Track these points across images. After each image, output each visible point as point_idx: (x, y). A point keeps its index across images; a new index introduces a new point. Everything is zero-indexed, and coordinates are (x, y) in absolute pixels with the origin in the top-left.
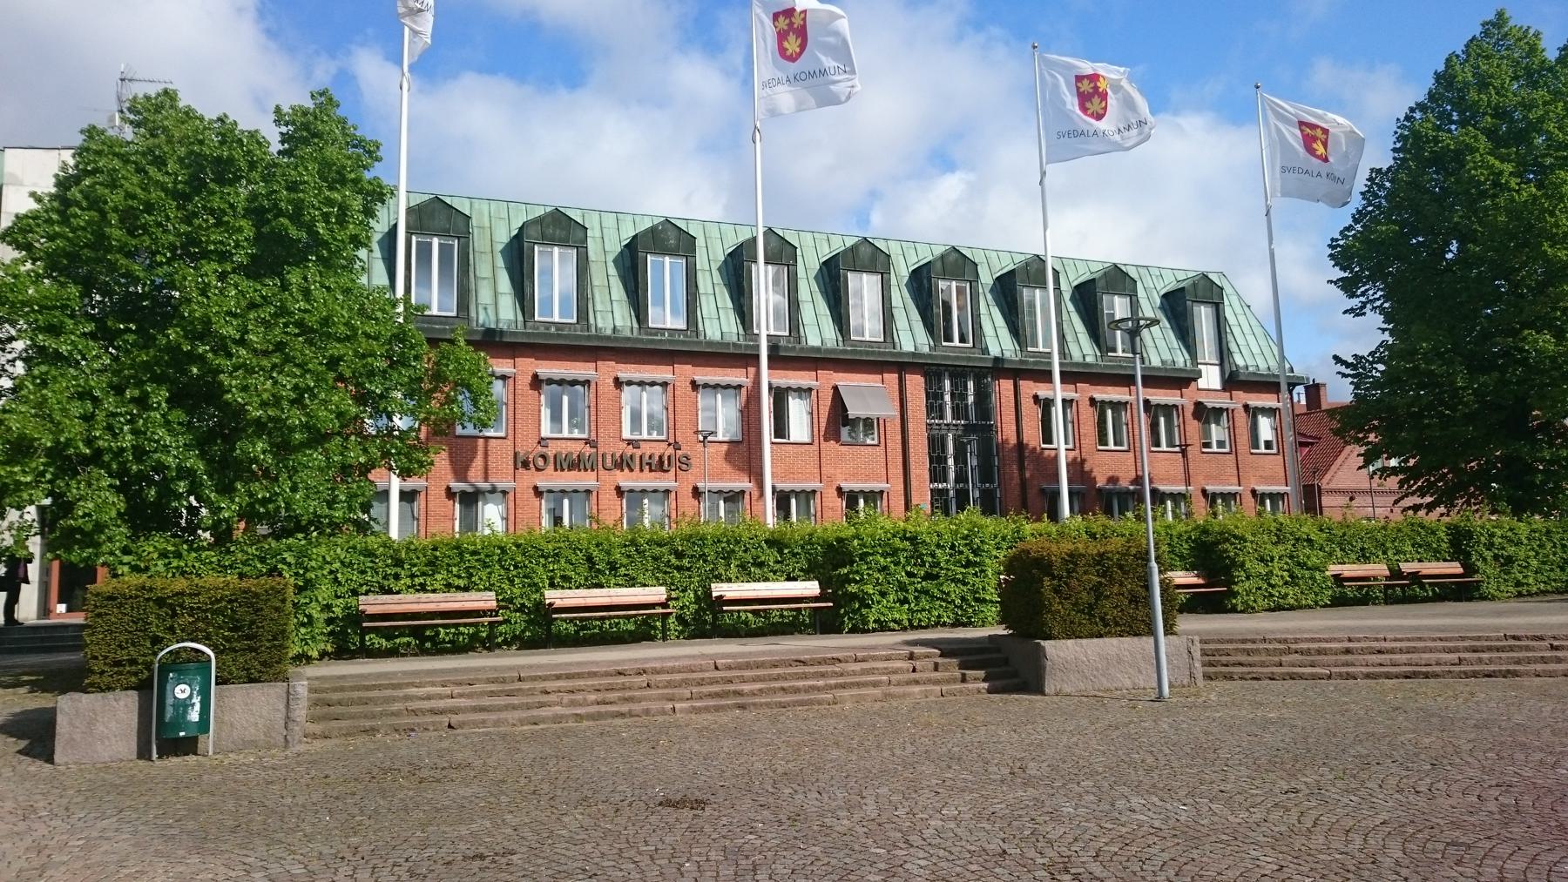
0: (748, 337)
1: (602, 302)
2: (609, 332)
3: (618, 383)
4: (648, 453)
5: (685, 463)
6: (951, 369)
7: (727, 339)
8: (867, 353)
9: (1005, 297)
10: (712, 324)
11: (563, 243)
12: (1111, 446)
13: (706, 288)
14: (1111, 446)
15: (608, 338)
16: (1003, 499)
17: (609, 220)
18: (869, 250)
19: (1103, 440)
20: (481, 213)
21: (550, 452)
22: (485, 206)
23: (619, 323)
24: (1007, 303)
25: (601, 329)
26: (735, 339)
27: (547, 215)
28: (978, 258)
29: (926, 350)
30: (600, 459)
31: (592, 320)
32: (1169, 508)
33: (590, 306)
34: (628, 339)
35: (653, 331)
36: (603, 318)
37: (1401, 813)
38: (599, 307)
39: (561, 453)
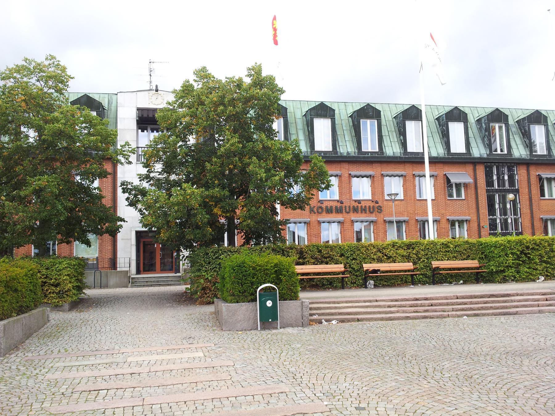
0: (405, 154)
1: (342, 142)
2: (345, 154)
3: (383, 176)
4: (363, 206)
5: (380, 209)
6: (497, 164)
7: (396, 155)
8: (459, 158)
9: (521, 130)
10: (389, 149)
11: (324, 116)
12: (455, 197)
13: (385, 133)
14: (455, 197)
15: (345, 157)
16: (522, 222)
17: (342, 106)
18: (458, 112)
19: (543, 194)
20: (290, 106)
21: (324, 206)
22: (291, 104)
23: (349, 150)
24: (522, 133)
25: (342, 153)
26: (399, 155)
27: (316, 106)
28: (467, 111)
29: (485, 156)
30: (344, 209)
31: (338, 150)
32: (466, 228)
33: (337, 143)
34: (354, 157)
35: (364, 153)
36: (343, 149)
37: (452, 398)
38: (340, 144)
39: (328, 206)
